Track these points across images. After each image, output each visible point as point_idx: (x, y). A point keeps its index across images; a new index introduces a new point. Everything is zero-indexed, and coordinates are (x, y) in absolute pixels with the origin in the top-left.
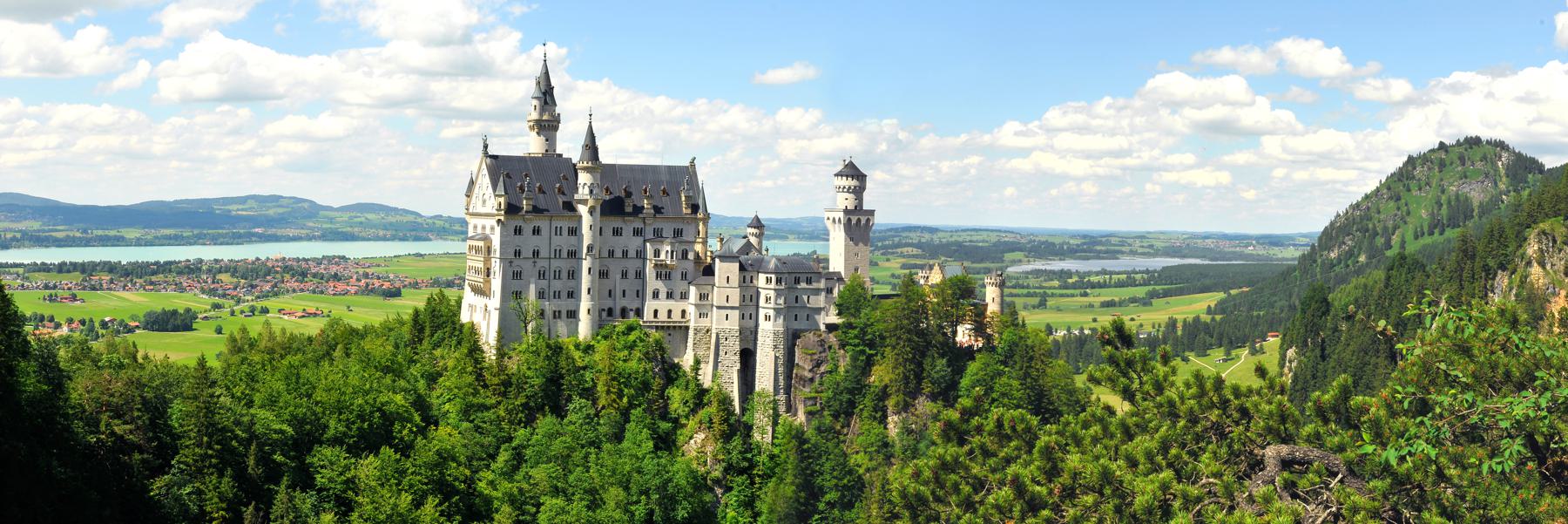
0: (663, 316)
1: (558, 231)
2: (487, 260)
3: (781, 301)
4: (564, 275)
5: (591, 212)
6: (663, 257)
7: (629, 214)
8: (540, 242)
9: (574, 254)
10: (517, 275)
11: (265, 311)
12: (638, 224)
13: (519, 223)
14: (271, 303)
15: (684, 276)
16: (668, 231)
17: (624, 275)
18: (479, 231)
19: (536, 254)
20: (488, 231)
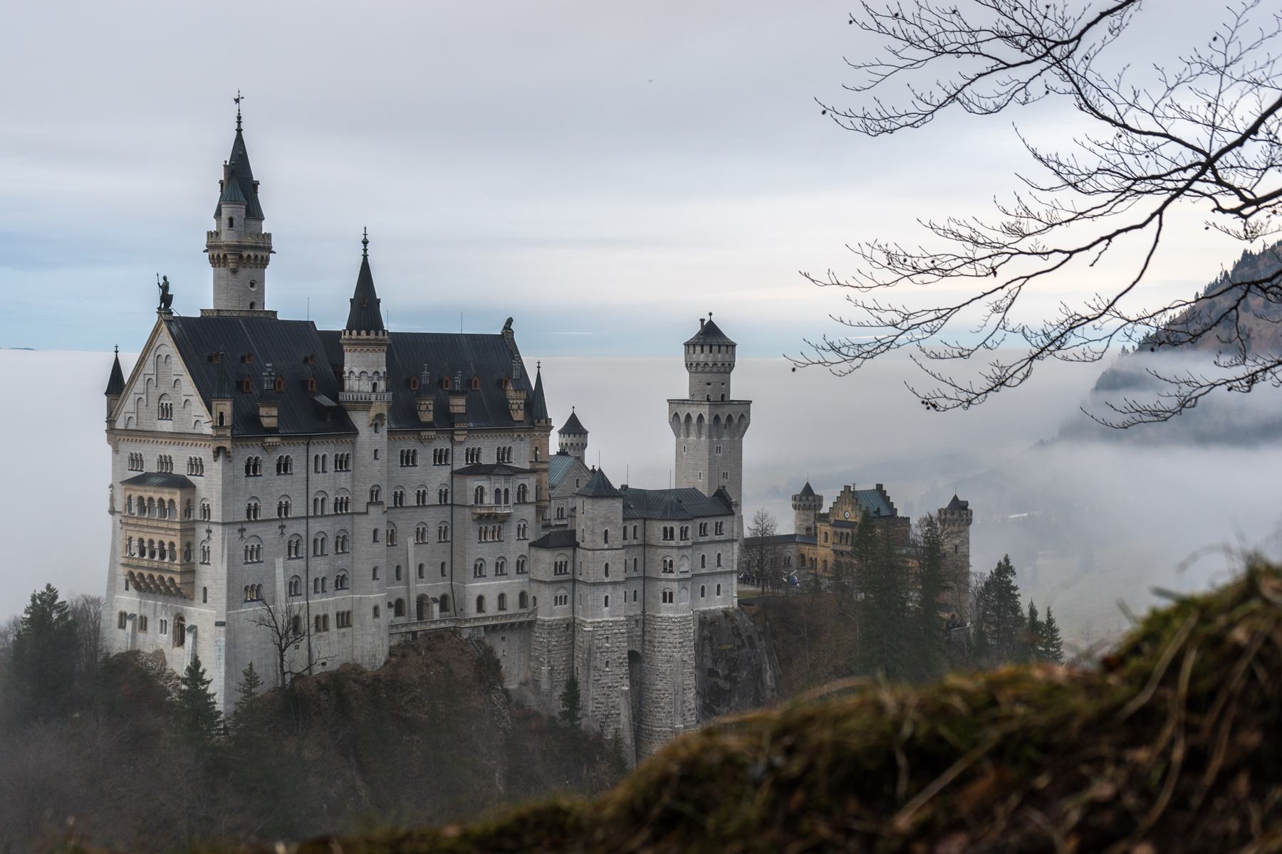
0: (491, 607)
1: (320, 464)
2: (188, 529)
4: (330, 546)
5: (376, 424)
6: (489, 499)
7: (428, 426)
8: (291, 488)
10: (253, 554)
12: (443, 444)
13: (254, 452)
16: (489, 458)
17: (421, 535)
18: (151, 466)
19: (284, 509)
20: (180, 469)
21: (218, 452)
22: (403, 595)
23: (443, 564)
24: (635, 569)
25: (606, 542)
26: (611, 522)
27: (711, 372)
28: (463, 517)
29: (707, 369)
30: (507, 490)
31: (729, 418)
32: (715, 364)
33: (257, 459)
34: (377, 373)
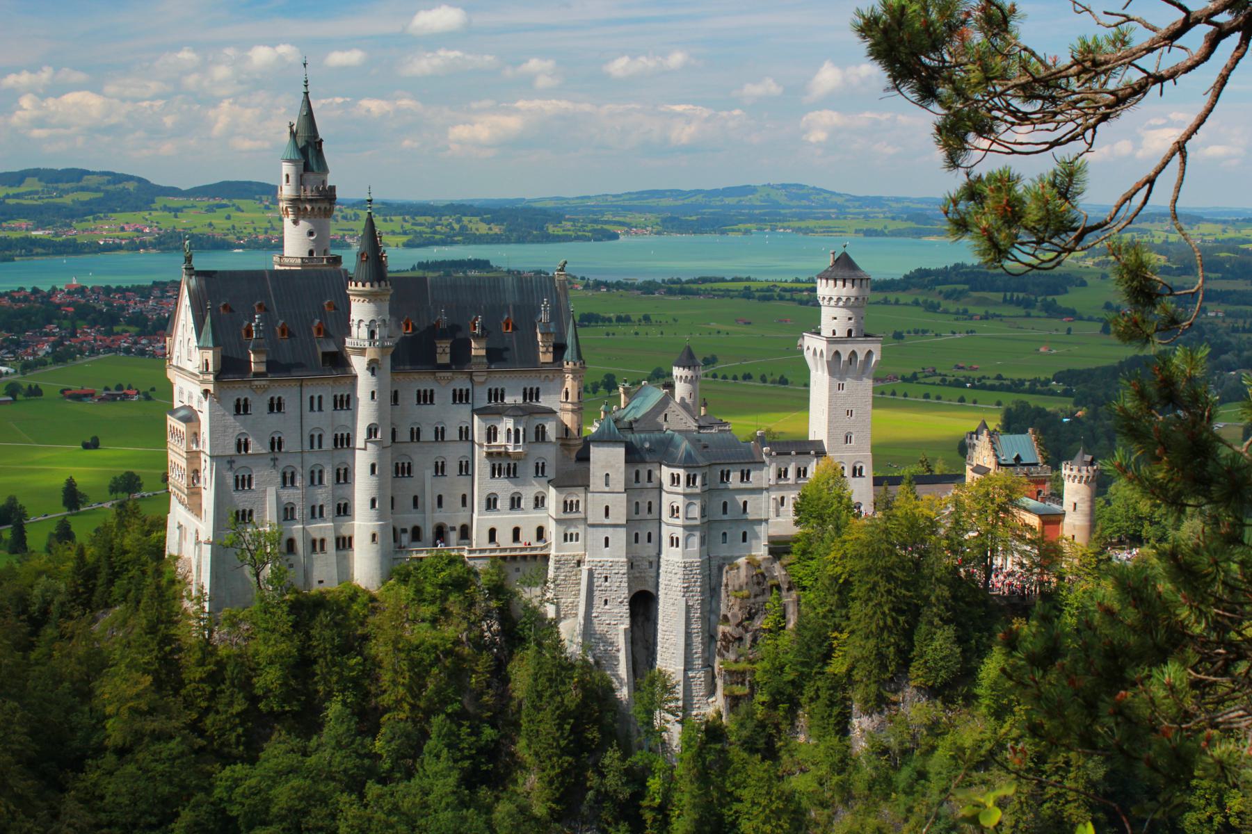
0: (505, 539)
1: (316, 404)
3: (696, 511)
4: (328, 477)
5: (373, 367)
6: (501, 439)
7: (445, 367)
8: (286, 425)
9: (344, 441)
10: (243, 483)
11: (35, 392)
12: (462, 383)
13: (243, 393)
14: (51, 380)
15: (540, 470)
17: (440, 469)
19: (276, 444)
21: (206, 392)
22: (419, 524)
23: (464, 497)
24: (650, 509)
25: (607, 485)
26: (612, 466)
27: (836, 306)
28: (480, 454)
29: (832, 303)
30: (517, 432)
31: (854, 353)
32: (839, 299)
33: (246, 400)
34: (372, 321)
